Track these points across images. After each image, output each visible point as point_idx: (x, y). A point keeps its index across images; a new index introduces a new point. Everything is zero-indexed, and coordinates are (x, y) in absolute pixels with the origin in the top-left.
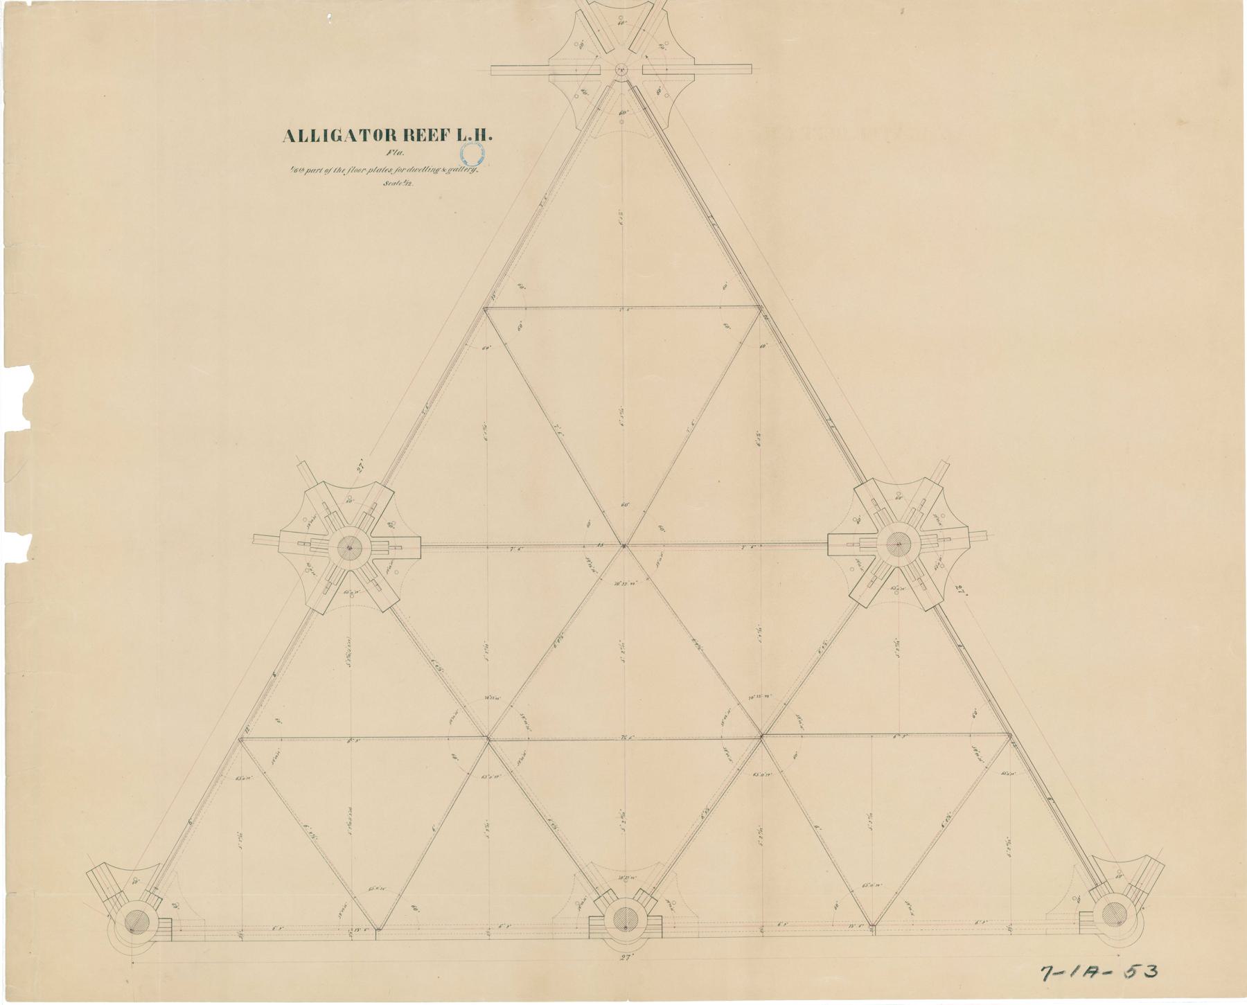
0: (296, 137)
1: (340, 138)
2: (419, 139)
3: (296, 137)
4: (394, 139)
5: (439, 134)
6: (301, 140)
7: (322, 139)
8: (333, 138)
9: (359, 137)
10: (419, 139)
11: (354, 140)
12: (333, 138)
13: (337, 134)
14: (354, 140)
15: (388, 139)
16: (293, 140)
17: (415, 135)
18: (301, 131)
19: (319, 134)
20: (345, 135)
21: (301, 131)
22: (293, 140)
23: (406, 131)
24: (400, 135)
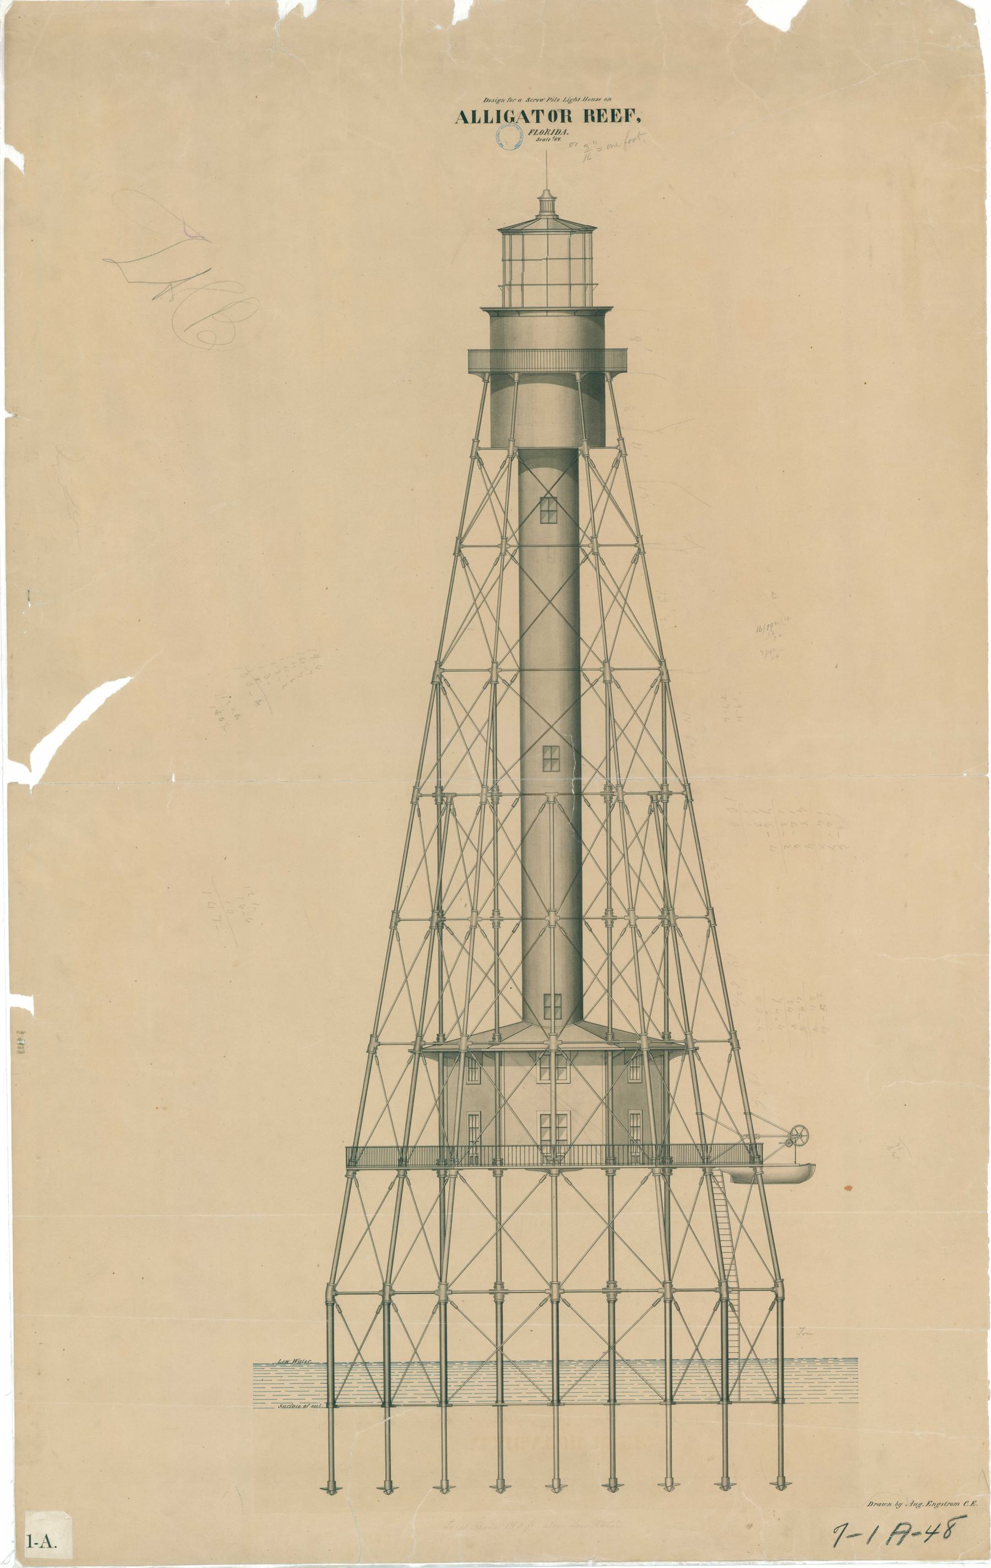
0: (469, 118)
1: (513, 119)
2: (599, 121)
3: (469, 118)
4: (569, 120)
5: (623, 114)
6: (474, 121)
7: (495, 120)
8: (506, 120)
9: (532, 118)
10: (599, 121)
11: (527, 121)
12: (506, 120)
13: (510, 115)
14: (527, 121)
15: (563, 121)
16: (466, 121)
17: (596, 115)
18: (474, 112)
19: (492, 115)
20: (517, 115)
21: (474, 112)
22: (466, 121)
23: (586, 111)
24: (578, 115)
